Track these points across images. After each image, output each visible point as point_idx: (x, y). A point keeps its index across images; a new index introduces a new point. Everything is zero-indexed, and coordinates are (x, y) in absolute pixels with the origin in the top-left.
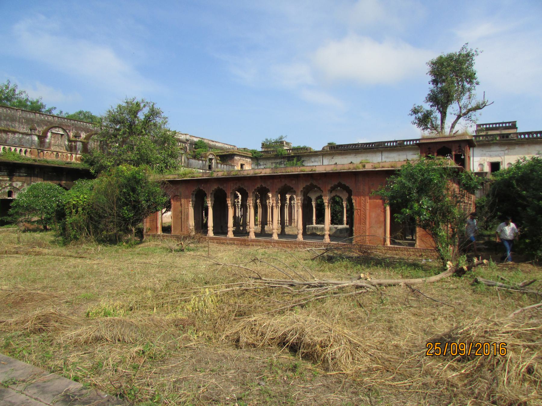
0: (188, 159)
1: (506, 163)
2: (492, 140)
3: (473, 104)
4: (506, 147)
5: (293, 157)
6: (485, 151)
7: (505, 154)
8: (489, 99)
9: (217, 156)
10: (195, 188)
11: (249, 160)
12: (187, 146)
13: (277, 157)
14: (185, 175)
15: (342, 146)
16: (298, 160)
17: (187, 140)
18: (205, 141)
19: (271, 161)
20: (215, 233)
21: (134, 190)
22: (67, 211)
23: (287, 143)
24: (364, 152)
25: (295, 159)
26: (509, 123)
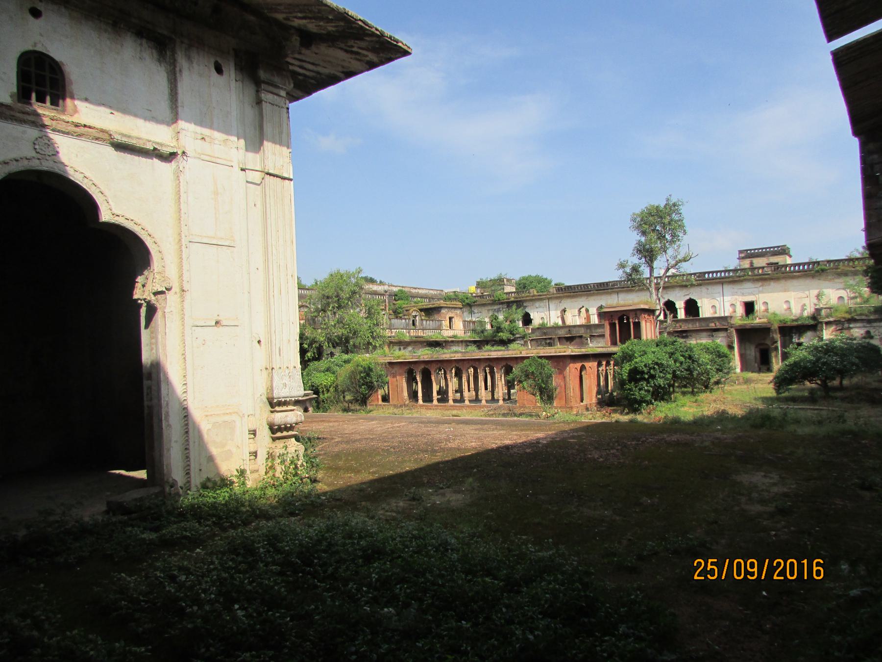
0: (390, 319)
1: (761, 302)
2: (744, 275)
3: (679, 257)
4: (760, 284)
5: (513, 302)
6: (736, 288)
7: (760, 292)
8: (694, 251)
9: (421, 310)
10: (407, 368)
11: (458, 312)
12: (386, 298)
13: (494, 303)
14: (399, 357)
15: (570, 287)
16: (518, 307)
17: (386, 292)
18: (406, 289)
19: (487, 308)
20: (424, 401)
21: (368, 375)
22: (321, 390)
23: (508, 280)
24: (597, 294)
25: (514, 307)
26: (778, 247)
